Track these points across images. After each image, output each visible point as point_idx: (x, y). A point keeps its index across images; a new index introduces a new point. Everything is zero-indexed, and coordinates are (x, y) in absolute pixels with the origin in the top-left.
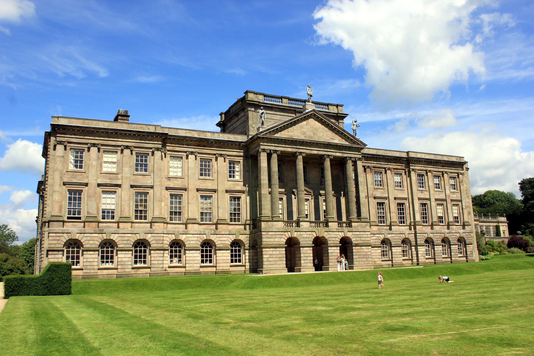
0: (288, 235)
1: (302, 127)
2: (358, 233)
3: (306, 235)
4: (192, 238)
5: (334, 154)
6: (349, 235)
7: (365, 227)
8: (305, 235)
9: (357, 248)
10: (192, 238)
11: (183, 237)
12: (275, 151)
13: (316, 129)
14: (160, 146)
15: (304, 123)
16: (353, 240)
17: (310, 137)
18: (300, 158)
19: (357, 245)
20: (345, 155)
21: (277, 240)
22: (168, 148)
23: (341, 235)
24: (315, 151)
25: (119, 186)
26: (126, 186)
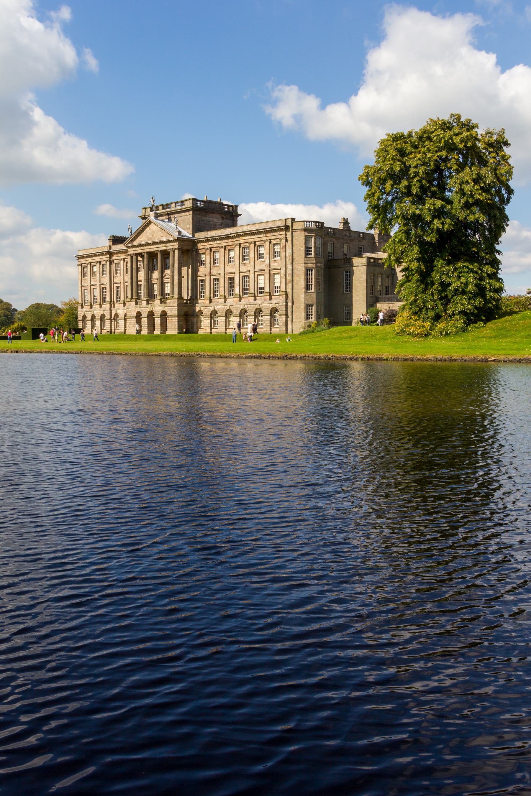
0: (137, 310)
2: (170, 308)
3: (145, 308)
6: (166, 309)
9: (170, 318)
11: (118, 312)
13: (153, 232)
14: (108, 259)
15: (148, 228)
16: (168, 313)
17: (151, 239)
19: (169, 317)
20: (169, 248)
21: (132, 313)
23: (161, 309)
24: (152, 249)
25: (96, 285)
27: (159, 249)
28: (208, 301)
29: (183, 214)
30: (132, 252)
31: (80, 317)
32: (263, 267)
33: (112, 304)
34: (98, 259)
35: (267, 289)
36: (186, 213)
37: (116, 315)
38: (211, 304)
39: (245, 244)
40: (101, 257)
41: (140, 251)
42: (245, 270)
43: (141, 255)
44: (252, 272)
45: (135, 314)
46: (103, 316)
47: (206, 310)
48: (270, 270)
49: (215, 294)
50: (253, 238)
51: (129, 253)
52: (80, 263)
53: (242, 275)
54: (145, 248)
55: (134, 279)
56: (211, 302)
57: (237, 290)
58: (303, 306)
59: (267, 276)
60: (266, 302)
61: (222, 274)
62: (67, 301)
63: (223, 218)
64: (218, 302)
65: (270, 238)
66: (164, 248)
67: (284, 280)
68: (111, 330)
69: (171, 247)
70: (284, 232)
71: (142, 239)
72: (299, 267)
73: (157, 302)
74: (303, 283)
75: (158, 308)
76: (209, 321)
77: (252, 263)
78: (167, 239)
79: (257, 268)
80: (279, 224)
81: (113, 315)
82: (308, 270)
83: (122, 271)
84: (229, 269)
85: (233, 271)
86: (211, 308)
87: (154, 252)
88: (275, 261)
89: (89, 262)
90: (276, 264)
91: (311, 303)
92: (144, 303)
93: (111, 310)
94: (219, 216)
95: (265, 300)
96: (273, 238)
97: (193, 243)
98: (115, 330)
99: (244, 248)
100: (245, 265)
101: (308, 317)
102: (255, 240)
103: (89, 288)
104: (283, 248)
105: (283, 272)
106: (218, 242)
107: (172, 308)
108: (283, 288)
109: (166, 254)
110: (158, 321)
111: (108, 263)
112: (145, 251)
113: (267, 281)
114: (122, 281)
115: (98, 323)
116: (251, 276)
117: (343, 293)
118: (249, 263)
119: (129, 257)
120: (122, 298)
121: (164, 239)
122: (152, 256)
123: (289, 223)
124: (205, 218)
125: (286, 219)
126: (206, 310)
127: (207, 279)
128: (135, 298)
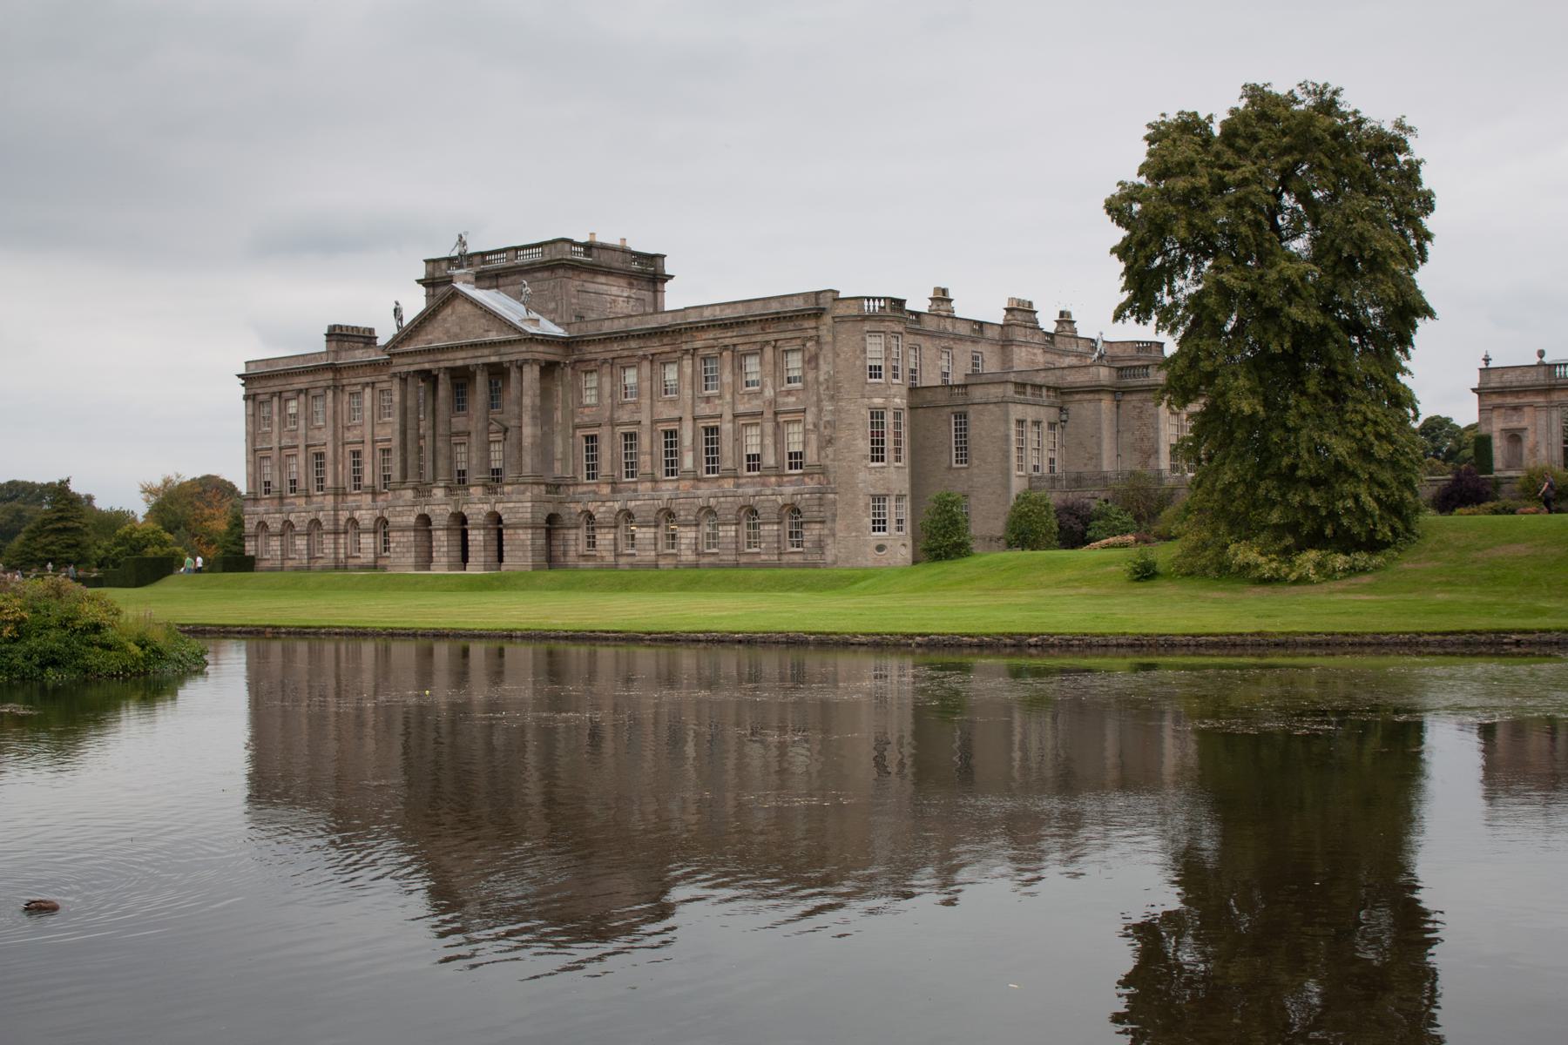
0: (418, 510)
1: (445, 320)
3: (440, 506)
4: (366, 517)
5: (486, 360)
6: (499, 508)
7: (523, 493)
8: (438, 510)
10: (366, 517)
11: (357, 514)
12: (408, 373)
13: (464, 319)
15: (449, 310)
17: (456, 336)
18: (441, 376)
19: (508, 527)
20: (505, 359)
22: (345, 382)
23: (487, 508)
24: (459, 360)
26: (302, 447)
27: (480, 361)
28: (606, 490)
29: (539, 275)
30: (405, 369)
31: (250, 526)
32: (755, 405)
33: (339, 492)
34: (301, 382)
35: (769, 460)
36: (546, 274)
37: (353, 522)
38: (618, 496)
39: (708, 351)
40: (311, 378)
41: (427, 366)
42: (708, 412)
43: (428, 377)
44: (728, 416)
45: (412, 520)
46: (316, 523)
47: (602, 509)
48: (776, 414)
49: (632, 469)
50: (729, 337)
51: (396, 370)
52: (251, 392)
53: (701, 424)
54: (440, 357)
55: (411, 434)
56: (614, 491)
57: (688, 462)
58: (863, 500)
59: (769, 427)
60: (769, 492)
61: (646, 420)
62: (158, 482)
63: (631, 285)
64: (635, 490)
65: (776, 336)
66: (494, 359)
67: (813, 437)
68: (336, 559)
69: (514, 358)
70: (812, 323)
71: (435, 337)
72: (852, 407)
73: (476, 492)
74: (864, 446)
75: (477, 507)
76: (611, 536)
77: (728, 397)
78: (503, 337)
79: (741, 409)
80: (800, 304)
81: (342, 522)
82: (877, 415)
83: (368, 414)
84: (666, 412)
85: (676, 414)
86: (617, 506)
87: (466, 367)
88: (789, 393)
89: (275, 389)
90: (792, 399)
91: (884, 492)
92: (439, 493)
93: (336, 510)
94: (623, 282)
95: (764, 485)
96: (782, 336)
97: (567, 344)
98: (347, 557)
99: (705, 359)
100: (708, 399)
101: (880, 525)
102: (735, 340)
103: (275, 454)
104: (809, 362)
105: (810, 418)
106: (633, 344)
107: (519, 506)
108: (811, 457)
109: (498, 373)
110: (476, 537)
111: (330, 394)
112: (442, 365)
113: (769, 441)
114: (368, 438)
115: (301, 543)
116: (727, 427)
117: (950, 468)
118: (720, 397)
119: (396, 381)
120: (367, 480)
121: (493, 336)
122: (461, 379)
123: (825, 302)
124: (591, 287)
125: (818, 293)
126: (602, 509)
127: (604, 433)
128: (412, 480)
